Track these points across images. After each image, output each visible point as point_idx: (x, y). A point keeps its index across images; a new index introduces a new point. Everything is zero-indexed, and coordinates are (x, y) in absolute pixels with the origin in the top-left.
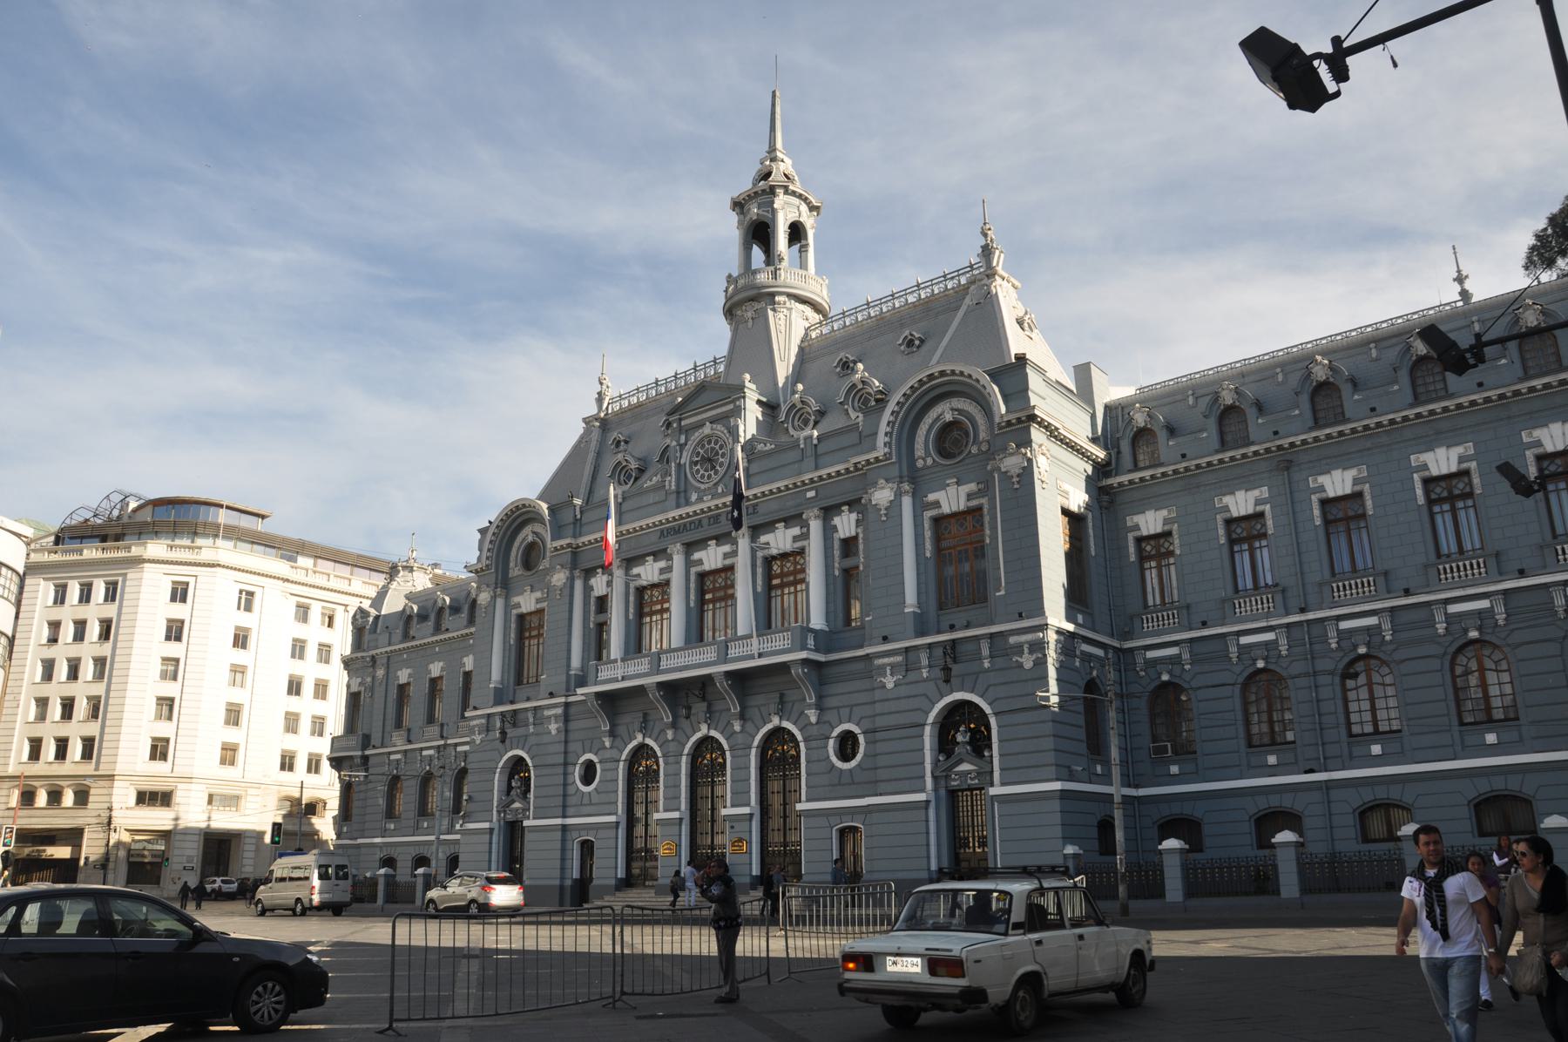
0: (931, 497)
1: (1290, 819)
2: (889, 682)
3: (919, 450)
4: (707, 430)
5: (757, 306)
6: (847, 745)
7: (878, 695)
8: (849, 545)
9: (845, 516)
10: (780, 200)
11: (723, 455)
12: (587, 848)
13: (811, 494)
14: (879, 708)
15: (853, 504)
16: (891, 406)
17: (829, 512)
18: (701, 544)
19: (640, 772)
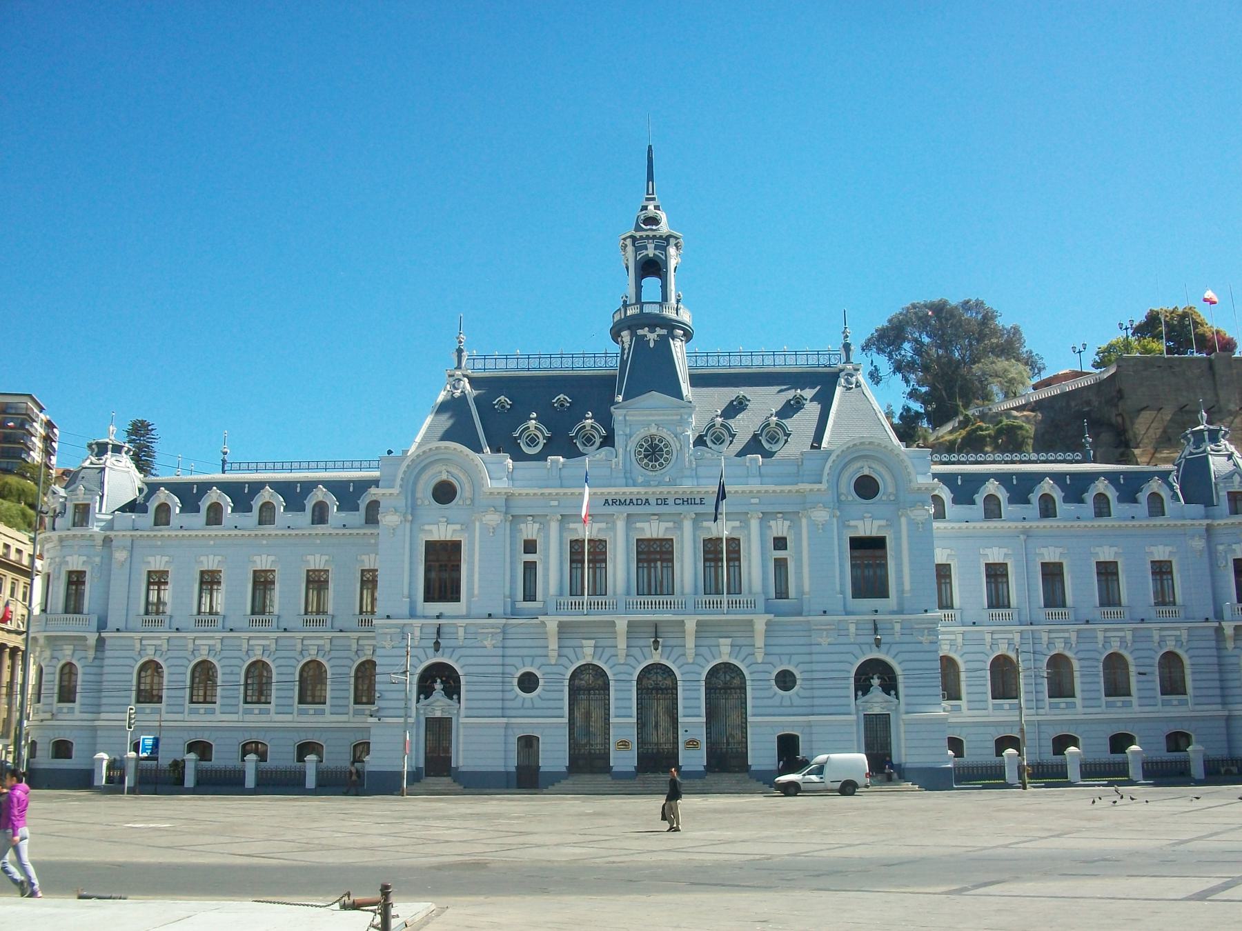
0: (852, 523)
1: (1073, 741)
2: (824, 641)
3: (843, 489)
4: (653, 431)
5: (659, 331)
6: (786, 680)
7: (815, 649)
8: (780, 543)
9: (780, 522)
10: (672, 250)
11: (668, 453)
12: (528, 743)
13: (753, 501)
14: (815, 658)
15: (792, 517)
16: (833, 457)
17: (766, 517)
18: (647, 517)
19: (589, 686)
